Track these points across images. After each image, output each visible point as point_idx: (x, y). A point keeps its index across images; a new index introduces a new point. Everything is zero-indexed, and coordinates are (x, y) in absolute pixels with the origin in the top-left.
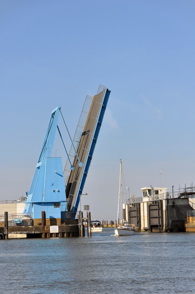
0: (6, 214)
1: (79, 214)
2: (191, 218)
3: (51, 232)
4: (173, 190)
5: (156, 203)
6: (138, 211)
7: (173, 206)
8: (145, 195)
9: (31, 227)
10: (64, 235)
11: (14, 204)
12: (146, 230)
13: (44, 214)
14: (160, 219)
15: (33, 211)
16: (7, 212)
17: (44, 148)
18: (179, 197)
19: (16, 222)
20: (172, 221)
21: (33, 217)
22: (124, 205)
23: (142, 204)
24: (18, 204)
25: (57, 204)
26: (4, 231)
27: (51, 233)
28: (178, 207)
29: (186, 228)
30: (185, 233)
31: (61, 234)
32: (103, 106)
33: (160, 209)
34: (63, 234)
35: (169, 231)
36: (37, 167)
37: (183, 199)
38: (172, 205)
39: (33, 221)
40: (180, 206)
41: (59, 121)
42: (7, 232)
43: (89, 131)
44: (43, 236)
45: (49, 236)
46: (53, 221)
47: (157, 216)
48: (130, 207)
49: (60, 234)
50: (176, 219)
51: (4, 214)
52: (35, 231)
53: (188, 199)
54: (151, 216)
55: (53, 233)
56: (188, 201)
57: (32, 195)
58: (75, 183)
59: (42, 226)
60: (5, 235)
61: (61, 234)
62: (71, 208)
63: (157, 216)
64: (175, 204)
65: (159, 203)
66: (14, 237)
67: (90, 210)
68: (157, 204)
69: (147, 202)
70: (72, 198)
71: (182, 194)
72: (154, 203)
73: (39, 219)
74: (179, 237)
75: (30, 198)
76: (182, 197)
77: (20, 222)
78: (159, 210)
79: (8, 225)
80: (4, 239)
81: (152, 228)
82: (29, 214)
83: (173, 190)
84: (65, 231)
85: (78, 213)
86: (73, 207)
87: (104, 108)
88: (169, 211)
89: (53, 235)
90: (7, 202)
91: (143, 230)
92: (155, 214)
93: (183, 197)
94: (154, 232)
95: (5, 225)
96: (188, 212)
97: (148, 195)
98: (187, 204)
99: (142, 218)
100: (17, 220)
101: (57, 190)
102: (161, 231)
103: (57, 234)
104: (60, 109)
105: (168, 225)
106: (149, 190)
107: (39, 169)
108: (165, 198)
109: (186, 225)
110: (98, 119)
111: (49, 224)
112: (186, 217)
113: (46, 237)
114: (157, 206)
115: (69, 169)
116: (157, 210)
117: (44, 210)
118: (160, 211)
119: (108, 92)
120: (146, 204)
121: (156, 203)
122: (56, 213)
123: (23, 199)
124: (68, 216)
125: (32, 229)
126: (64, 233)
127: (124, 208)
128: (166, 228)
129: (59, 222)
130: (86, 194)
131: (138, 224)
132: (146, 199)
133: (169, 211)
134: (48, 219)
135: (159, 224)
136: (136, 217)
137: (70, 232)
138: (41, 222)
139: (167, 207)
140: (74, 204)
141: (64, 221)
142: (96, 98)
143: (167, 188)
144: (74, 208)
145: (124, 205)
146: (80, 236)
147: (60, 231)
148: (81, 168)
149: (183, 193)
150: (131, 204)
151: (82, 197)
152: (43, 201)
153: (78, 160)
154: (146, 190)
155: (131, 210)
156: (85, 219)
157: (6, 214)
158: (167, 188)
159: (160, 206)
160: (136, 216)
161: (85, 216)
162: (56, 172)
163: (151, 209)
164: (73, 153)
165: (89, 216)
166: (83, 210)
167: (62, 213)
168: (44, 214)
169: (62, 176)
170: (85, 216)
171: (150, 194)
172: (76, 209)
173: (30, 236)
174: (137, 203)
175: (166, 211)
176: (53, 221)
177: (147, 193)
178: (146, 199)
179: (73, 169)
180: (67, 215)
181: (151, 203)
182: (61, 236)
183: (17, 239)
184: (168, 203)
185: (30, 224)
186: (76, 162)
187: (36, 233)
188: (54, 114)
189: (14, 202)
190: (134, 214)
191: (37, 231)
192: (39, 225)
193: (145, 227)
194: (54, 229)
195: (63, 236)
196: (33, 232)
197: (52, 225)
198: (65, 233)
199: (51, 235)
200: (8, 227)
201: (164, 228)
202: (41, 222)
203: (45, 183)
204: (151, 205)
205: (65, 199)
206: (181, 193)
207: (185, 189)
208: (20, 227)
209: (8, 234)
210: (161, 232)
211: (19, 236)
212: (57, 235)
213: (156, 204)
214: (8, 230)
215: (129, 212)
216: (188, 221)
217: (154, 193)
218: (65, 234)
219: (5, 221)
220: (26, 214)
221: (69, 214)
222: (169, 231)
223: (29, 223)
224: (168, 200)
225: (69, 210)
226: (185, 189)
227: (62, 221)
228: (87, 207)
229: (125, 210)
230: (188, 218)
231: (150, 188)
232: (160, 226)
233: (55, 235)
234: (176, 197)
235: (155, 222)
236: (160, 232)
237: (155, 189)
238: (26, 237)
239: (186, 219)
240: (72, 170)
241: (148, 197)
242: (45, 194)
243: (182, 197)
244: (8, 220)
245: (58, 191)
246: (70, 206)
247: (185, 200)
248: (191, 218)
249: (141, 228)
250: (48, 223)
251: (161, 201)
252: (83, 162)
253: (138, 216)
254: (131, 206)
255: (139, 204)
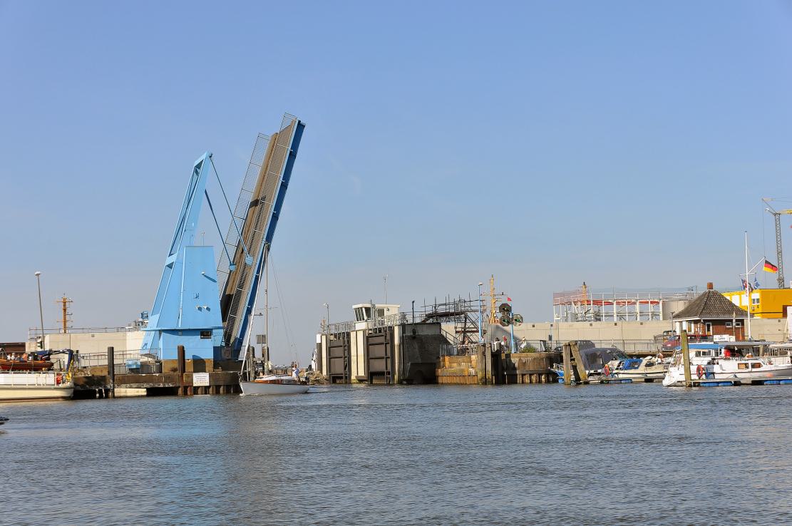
0: (111, 350)
2: (447, 358)
5: (380, 332)
6: (346, 348)
7: (414, 337)
8: (360, 318)
9: (157, 375)
10: (219, 391)
11: (120, 334)
12: (361, 381)
13: (182, 351)
14: (389, 361)
15: (161, 346)
16: (113, 348)
17: (181, 230)
18: (424, 321)
19: (129, 365)
20: (411, 364)
21: (161, 357)
22: (318, 336)
23: (353, 335)
24: (129, 334)
25: (205, 333)
26: (106, 384)
27: (195, 387)
28: (422, 340)
30: (436, 385)
31: (214, 389)
32: (291, 152)
34: (218, 387)
36: (168, 263)
38: (411, 336)
39: (161, 364)
40: (426, 336)
41: (208, 180)
43: (264, 198)
44: (180, 391)
45: (190, 392)
46: (199, 365)
47: (383, 354)
48: (330, 341)
50: (420, 361)
51: (107, 351)
53: (439, 324)
54: (371, 356)
55: (198, 387)
56: (440, 329)
57: (158, 316)
58: (239, 293)
59: (178, 373)
60: (107, 391)
61: (214, 389)
62: (232, 341)
63: (383, 354)
65: (386, 331)
66: (122, 394)
67: (270, 343)
68: (383, 333)
69: (364, 331)
70: (233, 320)
71: (429, 316)
72: (376, 332)
73: (173, 361)
74: (421, 395)
75: (153, 322)
76: (428, 322)
77: (137, 365)
78: (386, 344)
79: (113, 372)
80: (107, 397)
81: (372, 376)
82: (153, 352)
84: (221, 383)
86: (236, 339)
87: (293, 156)
88: (406, 345)
89: (199, 391)
92: (379, 351)
93: (431, 320)
94: (377, 385)
97: (365, 318)
98: (437, 333)
99: (353, 359)
100: (130, 363)
101: (205, 307)
103: (206, 387)
104: (210, 157)
105: (403, 372)
106: (368, 310)
107: (171, 268)
108: (398, 323)
109: (440, 370)
110: (282, 176)
112: (439, 358)
113: (185, 393)
114: (384, 337)
115: (226, 268)
116: (382, 344)
117: (181, 344)
118: (388, 346)
119: (301, 127)
120: (360, 335)
121: (380, 332)
122: (204, 349)
123: (139, 325)
124: (226, 355)
126: (220, 386)
127: (318, 341)
129: (209, 366)
131: (345, 369)
132: (361, 326)
133: (406, 345)
135: (387, 369)
137: (230, 386)
138: (176, 365)
139: (402, 339)
140: (236, 333)
142: (276, 139)
143: (399, 306)
150: (332, 334)
151: (251, 318)
152: (180, 327)
153: (243, 250)
154: (361, 308)
156: (259, 359)
157: (111, 350)
158: (399, 306)
159: (388, 337)
161: (258, 354)
164: (234, 239)
167: (215, 348)
168: (182, 351)
169: (214, 281)
171: (369, 316)
172: (240, 342)
173: (152, 392)
175: (400, 346)
176: (199, 365)
177: (363, 315)
178: (361, 326)
179: (233, 268)
181: (370, 332)
182: (214, 392)
183: (127, 397)
184: (404, 332)
185: (157, 369)
188: (199, 166)
190: (338, 352)
192: (172, 371)
193: (359, 375)
194: (201, 379)
195: (218, 392)
196: (161, 386)
197: (196, 371)
199: (196, 390)
200: (114, 375)
201: (396, 377)
202: (176, 365)
204: (371, 335)
205: (220, 324)
206: (427, 313)
207: (435, 307)
208: (137, 374)
210: (390, 384)
212: (206, 390)
213: (380, 334)
214: (114, 380)
215: (329, 349)
218: (222, 389)
220: (147, 352)
223: (154, 369)
224: (403, 326)
225: (227, 344)
226: (435, 307)
227: (216, 365)
228: (262, 339)
229: (321, 344)
230: (441, 358)
231: (368, 305)
232: (389, 373)
234: (418, 321)
235: (379, 366)
236: (389, 384)
237: (378, 306)
238: (145, 394)
239: (438, 360)
240: (231, 271)
242: (182, 314)
243: (428, 322)
245: (208, 309)
246: (230, 336)
247: (434, 326)
248: (447, 358)
250: (189, 368)
251: (391, 329)
252: (253, 256)
253: (346, 354)
254: (332, 338)
255: (348, 334)
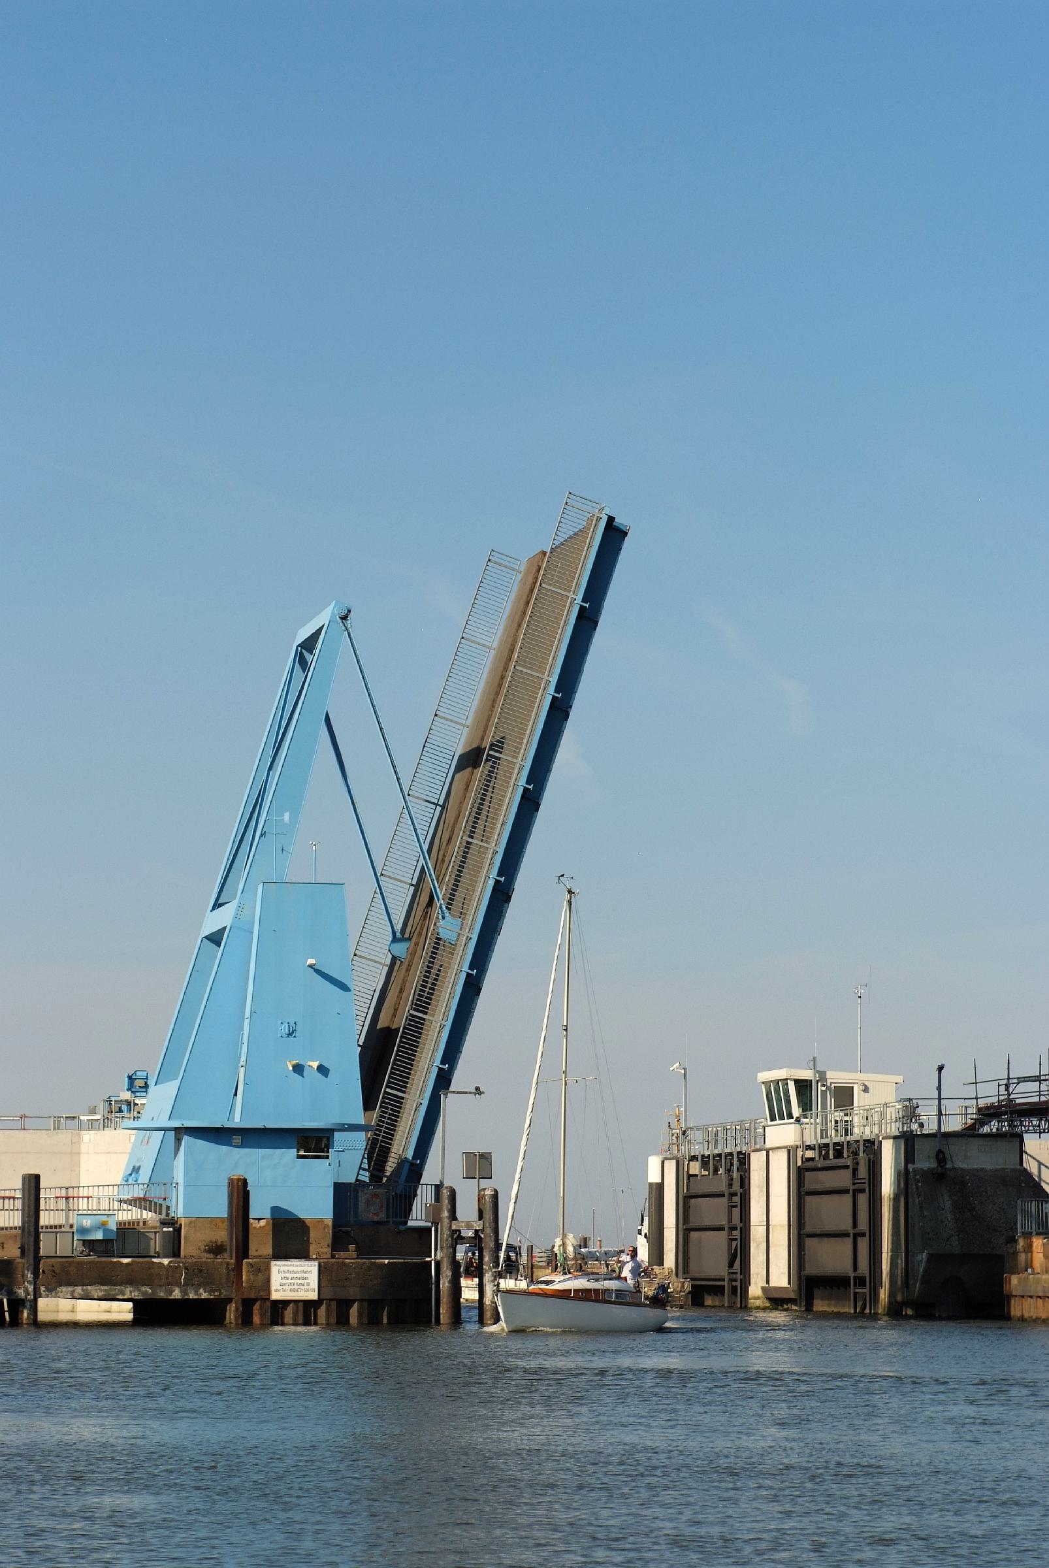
0: (33, 1184)
1: (431, 1200)
3: (275, 1296)
4: (939, 1088)
5: (839, 1154)
6: (737, 1199)
8: (778, 1113)
9: (166, 1261)
11: (63, 1137)
12: (776, 1301)
13: (240, 1193)
14: (863, 1244)
15: (179, 1174)
16: (37, 1178)
19: (83, 1230)
20: (930, 1256)
21: (179, 1210)
22: (654, 1163)
23: (757, 1162)
24: (88, 1136)
29: (1009, 1297)
32: (582, 608)
33: (863, 1191)
35: (910, 1312)
37: (989, 1136)
38: (931, 1170)
39: (178, 1231)
42: (31, 1288)
43: (498, 745)
44: (231, 1313)
45: (262, 1316)
47: (846, 1224)
48: (690, 1176)
49: (323, 1308)
50: (955, 1246)
51: (19, 1184)
52: (187, 1283)
54: (808, 1229)
55: (285, 1303)
56: (1021, 1152)
57: (177, 1083)
58: (416, 1027)
59: (228, 1258)
60: (17, 1305)
62: (391, 1165)
63: (846, 1224)
64: (949, 1166)
65: (856, 1154)
66: (64, 1317)
69: (791, 1152)
70: (395, 1107)
71: (988, 1113)
72: (826, 1157)
73: (212, 1221)
76: (986, 1129)
77: (106, 1231)
78: (856, 1192)
79: (37, 1248)
80: (15, 1323)
82: (156, 1193)
83: (939, 1088)
84: (353, 1292)
85: (424, 1198)
86: (402, 1162)
87: (587, 621)
89: (289, 1313)
90: (23, 1122)
91: (758, 1303)
93: (992, 1127)
95: (22, 1248)
96: (1027, 1214)
97: (796, 1111)
98: (1012, 1163)
100: (87, 1222)
101: (315, 1065)
102: (864, 1307)
103: (307, 1304)
104: (344, 618)
105: (904, 1278)
106: (803, 1087)
107: (218, 944)
108: (894, 1129)
109: (1015, 1280)
110: (554, 679)
111: (268, 1250)
112: (1013, 1240)
113: (246, 1320)
114: (849, 1173)
117: (238, 1173)
118: (863, 1199)
119: (614, 535)
120: (780, 1166)
121: (839, 1154)
124: (371, 1210)
125: (170, 1279)
126: (349, 1303)
127: (654, 1177)
128: (892, 1294)
129: (320, 1242)
130: (478, 1091)
131: (731, 1265)
132: (783, 1134)
134: (263, 1223)
135: (855, 1268)
136: (721, 1229)
139: (904, 1177)
140: (403, 1145)
141: (348, 1234)
143: (900, 1079)
144: (406, 1167)
145: (654, 1163)
146: (438, 1322)
147: (327, 1294)
148: (454, 946)
149: (992, 1106)
150: (693, 1158)
151: (450, 1104)
152: (237, 1121)
155: (693, 1191)
157: (33, 1184)
158: (900, 1079)
159: (863, 1172)
160: (724, 1222)
161: (467, 1211)
162: (311, 961)
163: (808, 1186)
165: (488, 1215)
166: (455, 1177)
167: (341, 1190)
168: (240, 1193)
169: (344, 987)
170: (467, 1211)
172: (413, 1170)
174: (731, 1154)
175: (896, 1199)
177: (788, 1102)
178: (783, 1134)
179: (401, 949)
180: (368, 1203)
182: (333, 1321)
183: (76, 1325)
184: (910, 1156)
185: (163, 1246)
186: (419, 913)
187: (192, 1296)
188: (309, 644)
189: (67, 1121)
190: (713, 1211)
191: (199, 1286)
192: (209, 1251)
193: (774, 1283)
195: (342, 1321)
196: (177, 1294)
197: (281, 1254)
198: (353, 1301)
199: (277, 1311)
200: (37, 1258)
201: (884, 1294)
203: (247, 1022)
204: (810, 1164)
205: (358, 1115)
207: (1007, 1086)
209: (35, 1300)
210: (864, 1314)
211: (90, 1310)
212: (307, 1311)
216: (1022, 1257)
217: (831, 1102)
218: (354, 1310)
219: (22, 1228)
221: (376, 1195)
222: (910, 1312)
223: (157, 1244)
224: (908, 1141)
226: (1007, 1086)
227: (341, 1236)
229: (660, 1187)
230: (1021, 1243)
231: (806, 1074)
232: (861, 1281)
233: (296, 1313)
234: (954, 1124)
236: (859, 1315)
237: (836, 1077)
238: (130, 1317)
240: (394, 959)
241: (798, 1120)
242: (246, 1084)
243: (986, 1129)
244: (42, 1222)
245: (323, 1070)
246: (385, 1153)
249: (747, 1291)
250: (260, 1245)
251: (872, 1147)
253: (736, 1220)
254: (695, 1168)
255: (744, 1160)
